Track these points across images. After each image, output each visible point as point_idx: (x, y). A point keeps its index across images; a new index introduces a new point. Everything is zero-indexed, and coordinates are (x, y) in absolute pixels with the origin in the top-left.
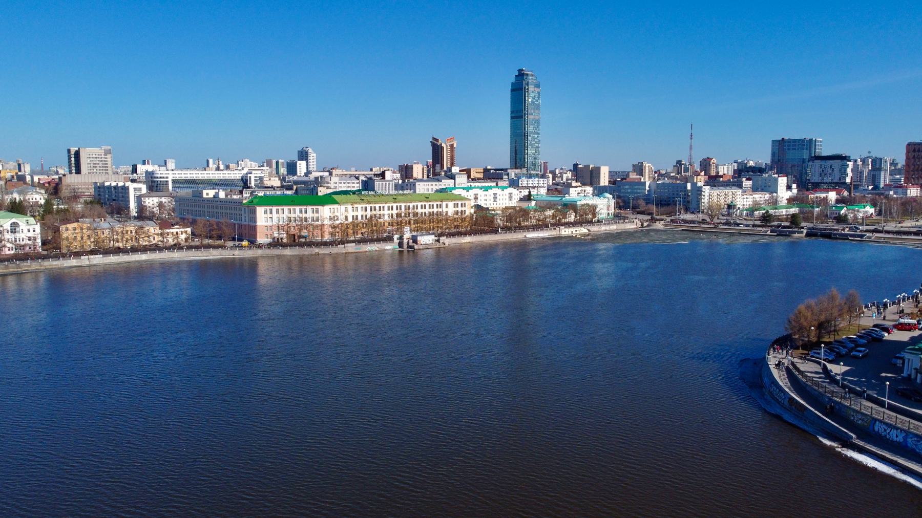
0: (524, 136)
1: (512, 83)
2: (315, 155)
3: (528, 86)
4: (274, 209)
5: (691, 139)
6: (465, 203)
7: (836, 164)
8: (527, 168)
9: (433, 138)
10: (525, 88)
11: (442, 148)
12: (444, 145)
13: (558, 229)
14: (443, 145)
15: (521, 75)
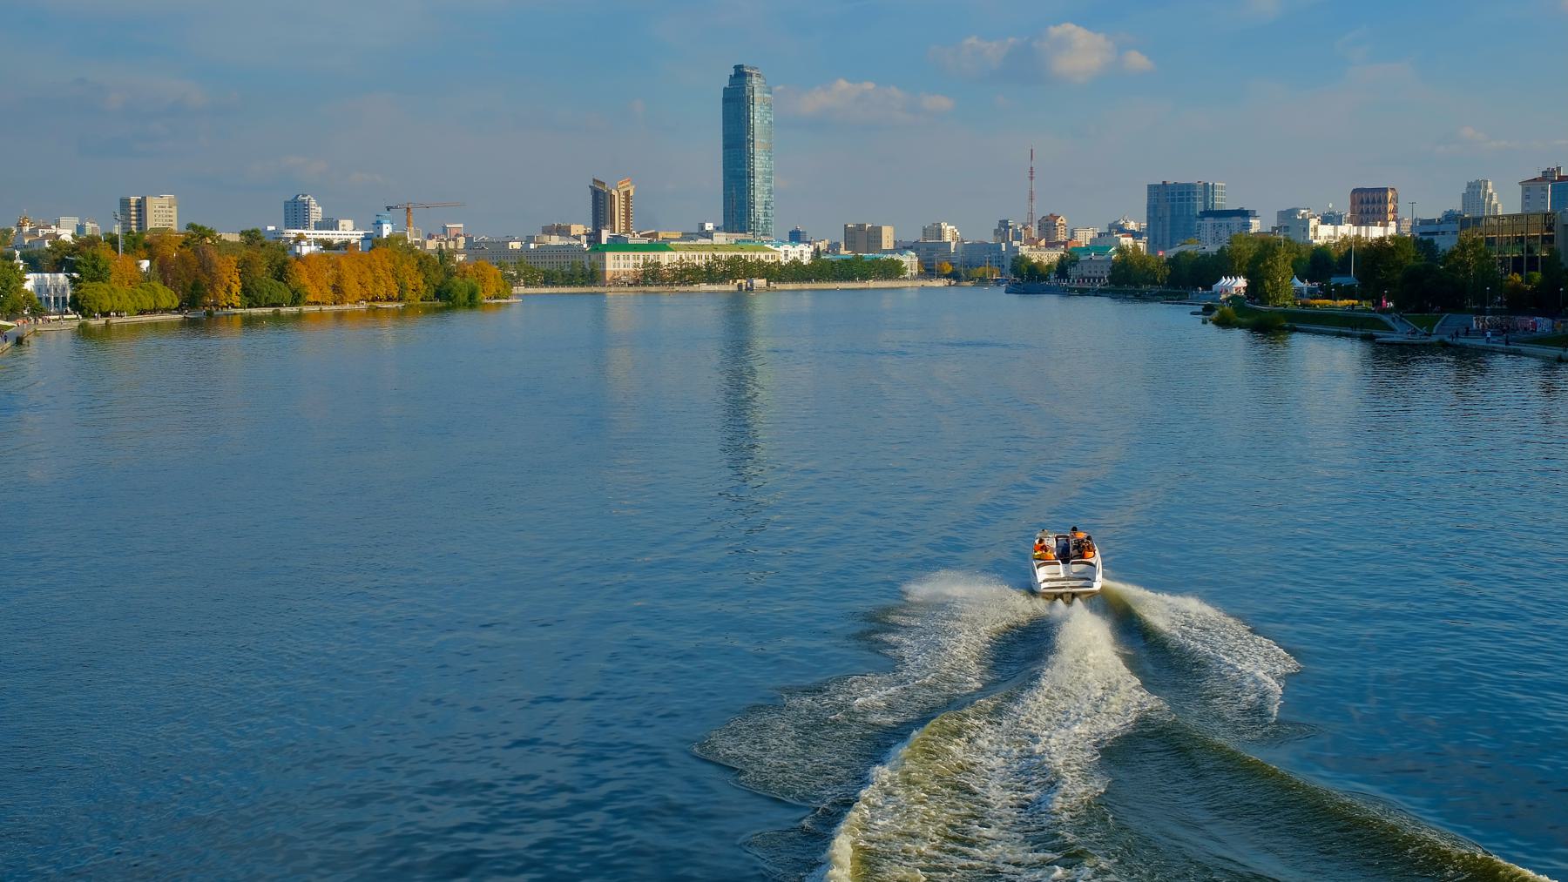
0: (749, 177)
1: (725, 89)
2: (320, 209)
3: (753, 95)
4: (621, 255)
5: (1032, 178)
7: (1237, 220)
8: (754, 230)
9: (594, 180)
10: (749, 97)
11: (612, 197)
12: (614, 192)
15: (740, 74)
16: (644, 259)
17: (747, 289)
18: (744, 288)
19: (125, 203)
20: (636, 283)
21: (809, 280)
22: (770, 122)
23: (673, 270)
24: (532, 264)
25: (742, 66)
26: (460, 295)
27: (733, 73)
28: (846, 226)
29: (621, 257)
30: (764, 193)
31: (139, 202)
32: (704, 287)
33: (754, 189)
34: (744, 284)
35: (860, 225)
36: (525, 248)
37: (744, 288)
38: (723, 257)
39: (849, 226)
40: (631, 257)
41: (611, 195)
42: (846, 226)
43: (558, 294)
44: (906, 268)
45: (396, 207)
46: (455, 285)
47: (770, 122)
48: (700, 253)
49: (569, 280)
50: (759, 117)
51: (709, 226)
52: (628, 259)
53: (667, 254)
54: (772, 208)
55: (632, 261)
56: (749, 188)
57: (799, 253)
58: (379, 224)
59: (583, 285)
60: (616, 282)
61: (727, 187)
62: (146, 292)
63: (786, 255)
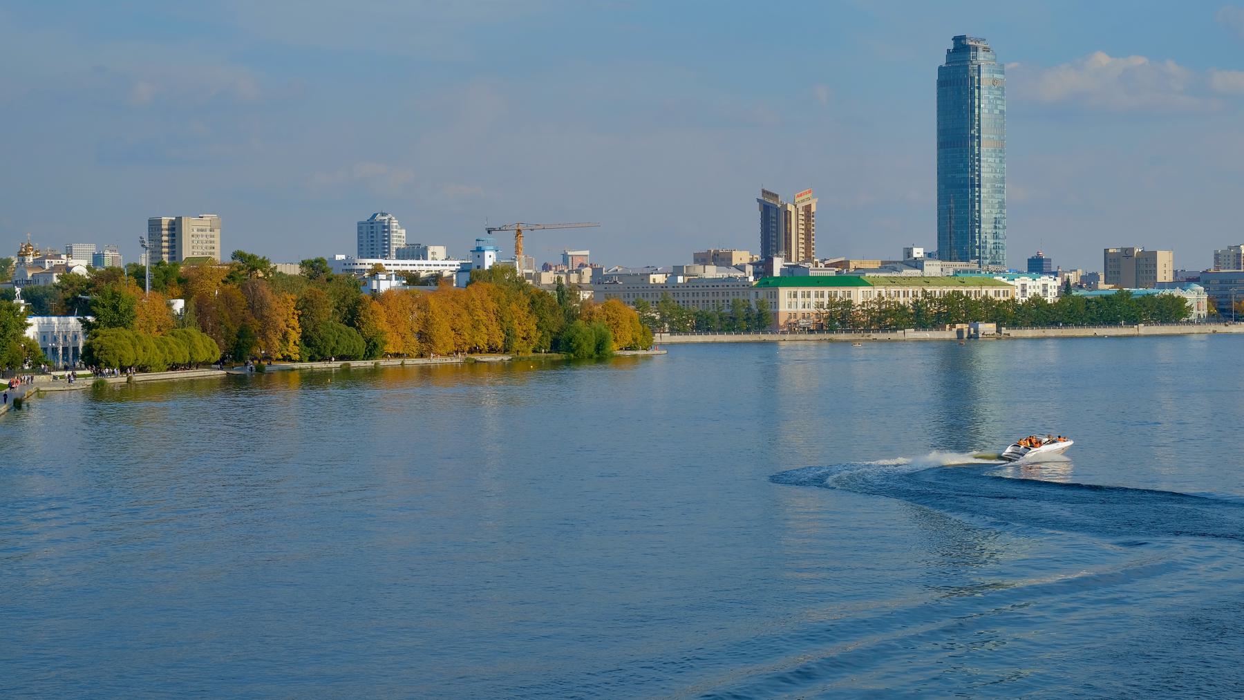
0: (973, 186)
1: (940, 68)
2: (403, 232)
3: (979, 76)
4: (800, 291)
6: (1007, 291)
8: (979, 257)
9: (764, 192)
10: (972, 79)
11: (787, 213)
12: (790, 208)
13: (1136, 327)
14: (789, 209)
15: (961, 49)
16: (830, 296)
17: (970, 337)
18: (966, 335)
19: (155, 225)
20: (820, 329)
21: (1054, 324)
22: (1002, 112)
23: (869, 312)
24: (681, 303)
25: (964, 37)
26: (585, 345)
27: (951, 47)
28: (1106, 251)
29: (799, 294)
30: (993, 207)
31: (172, 223)
32: (911, 334)
33: (979, 202)
34: (966, 330)
35: (1127, 249)
36: (670, 285)
37: (966, 335)
38: (938, 293)
39: (1111, 251)
40: (813, 294)
41: (786, 212)
42: (1106, 251)
43: (714, 343)
44: (1190, 308)
45: (500, 229)
46: (578, 332)
47: (1002, 112)
48: (906, 289)
49: (730, 324)
50: (987, 105)
51: (918, 252)
52: (809, 296)
53: (861, 289)
54: (1004, 227)
55: (813, 300)
56: (973, 200)
57: (1041, 288)
58: (480, 251)
59: (748, 331)
60: (792, 328)
61: (943, 199)
62: (179, 341)
63: (1024, 291)
